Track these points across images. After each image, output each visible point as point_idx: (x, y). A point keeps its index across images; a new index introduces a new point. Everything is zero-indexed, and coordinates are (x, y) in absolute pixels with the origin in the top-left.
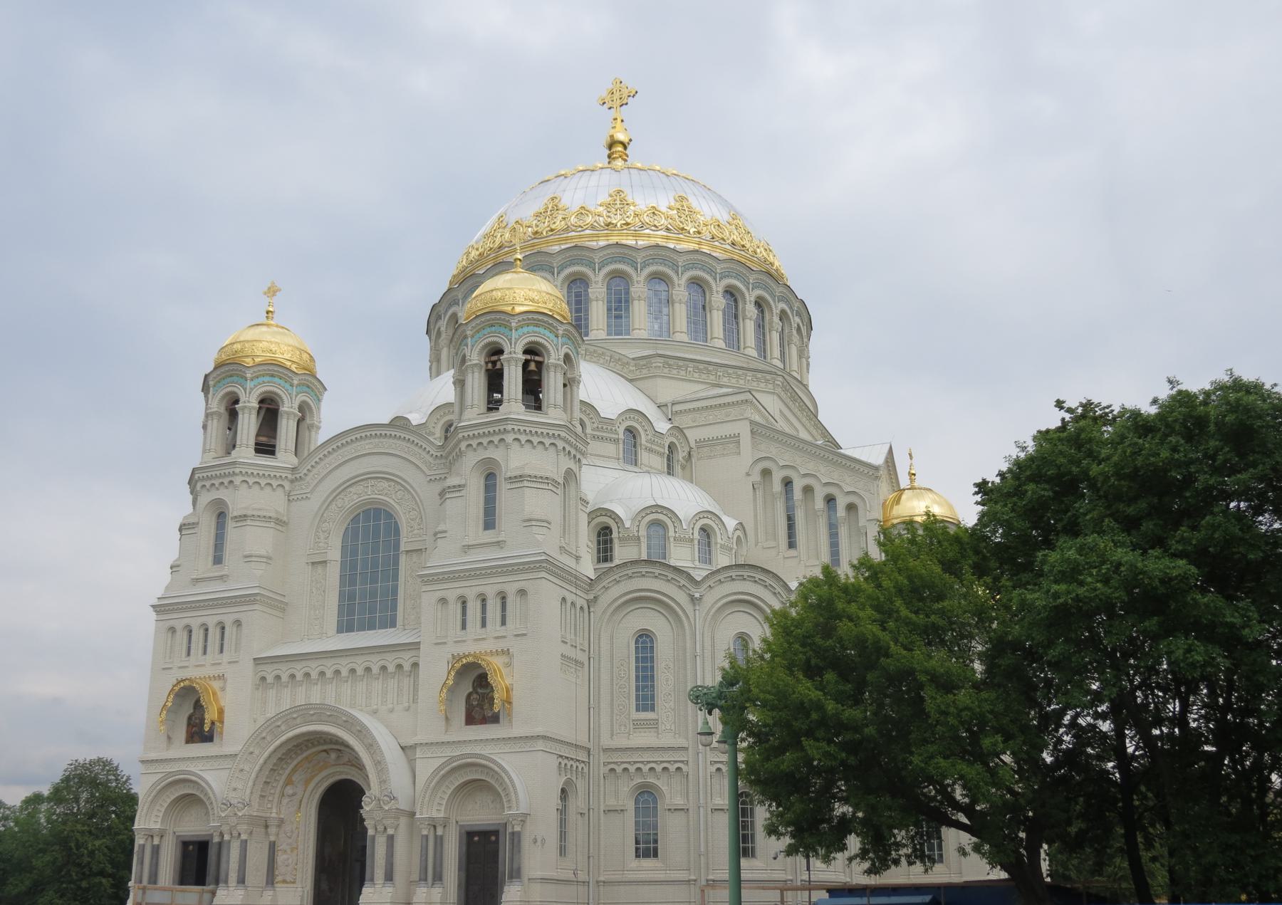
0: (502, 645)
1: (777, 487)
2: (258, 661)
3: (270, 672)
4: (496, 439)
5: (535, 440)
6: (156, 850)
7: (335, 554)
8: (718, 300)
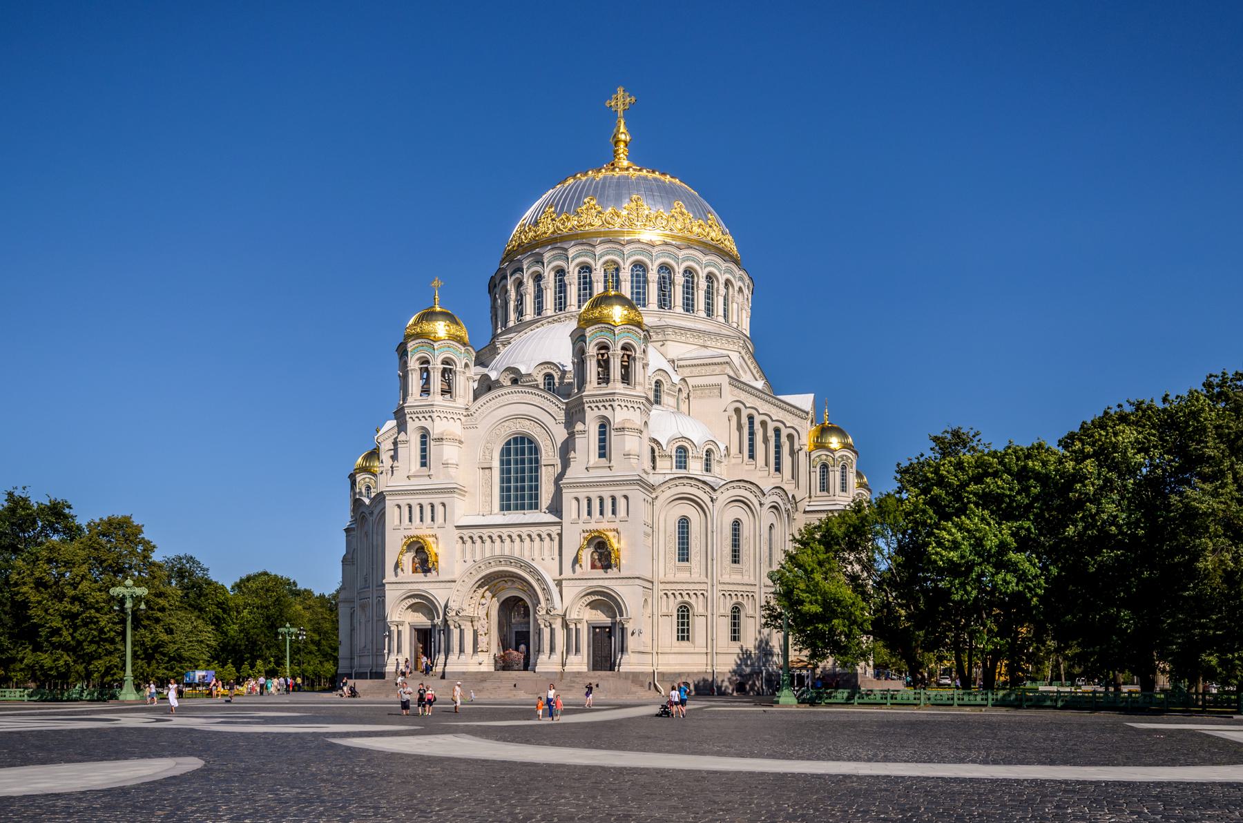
0: (613, 526)
1: (745, 420)
2: (458, 527)
3: (466, 533)
4: (607, 404)
5: (629, 405)
6: (399, 633)
7: (496, 464)
8: (703, 284)
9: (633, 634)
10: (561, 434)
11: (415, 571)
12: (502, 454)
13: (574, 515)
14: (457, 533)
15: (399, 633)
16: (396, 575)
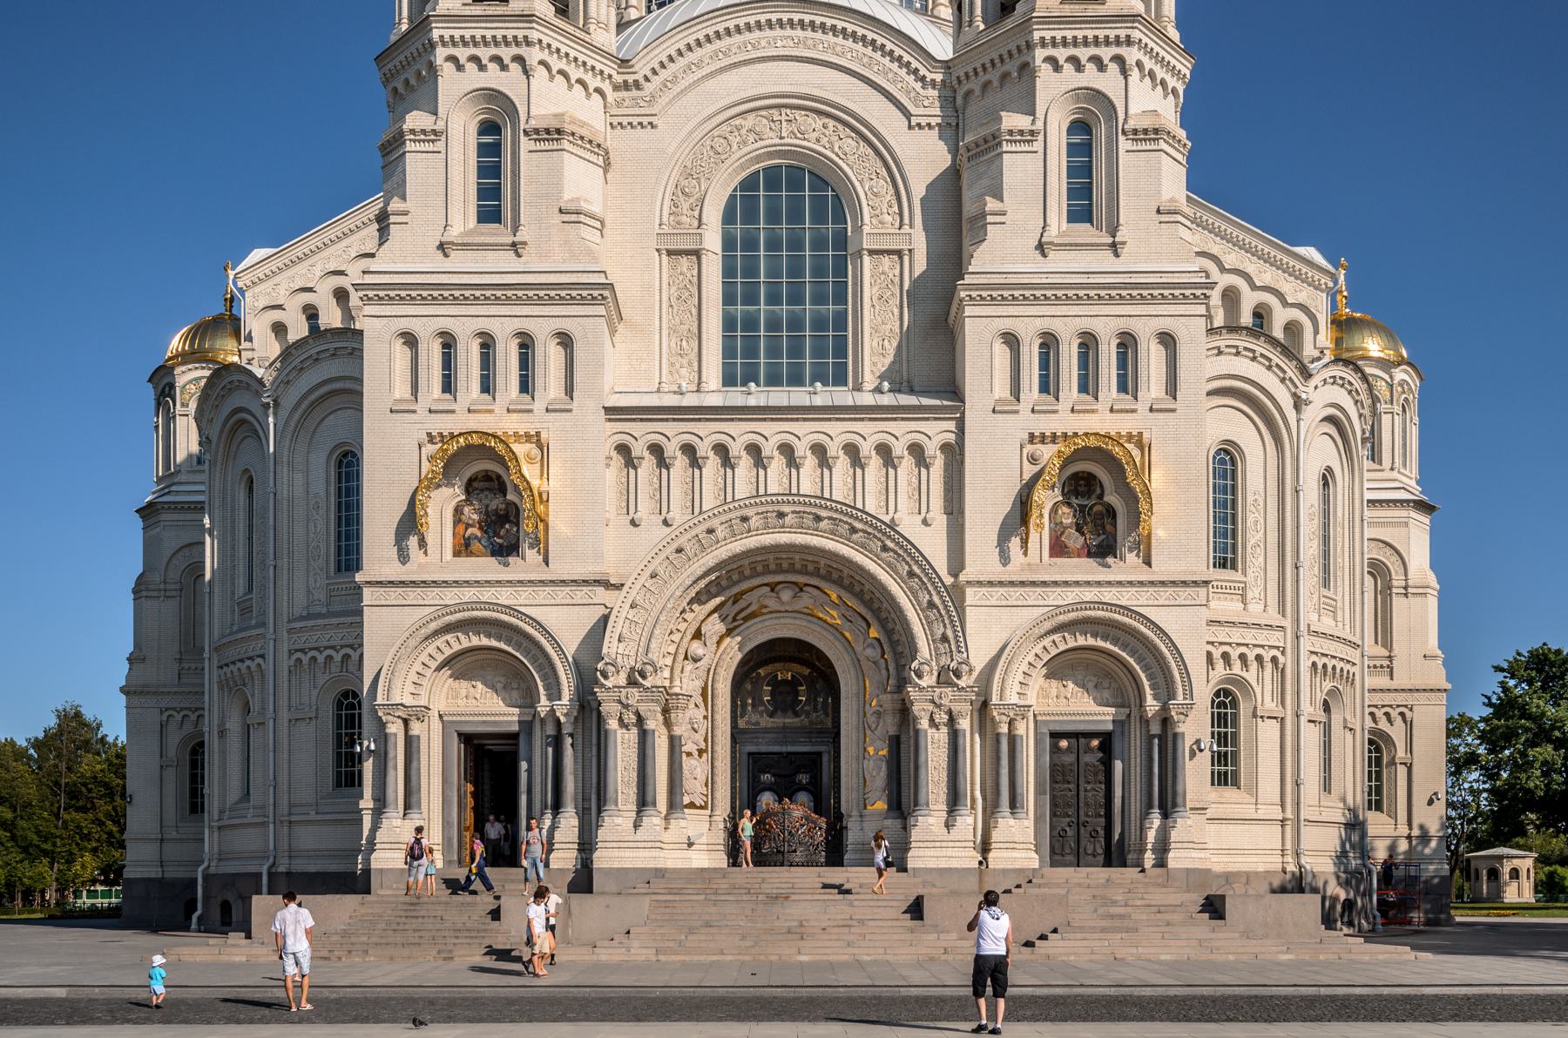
3: (641, 434)
6: (410, 742)
7: (713, 241)
9: (1193, 755)
10: (925, 157)
11: (464, 548)
12: (728, 217)
13: (1002, 389)
14: (608, 434)
15: (410, 742)
16: (403, 557)
